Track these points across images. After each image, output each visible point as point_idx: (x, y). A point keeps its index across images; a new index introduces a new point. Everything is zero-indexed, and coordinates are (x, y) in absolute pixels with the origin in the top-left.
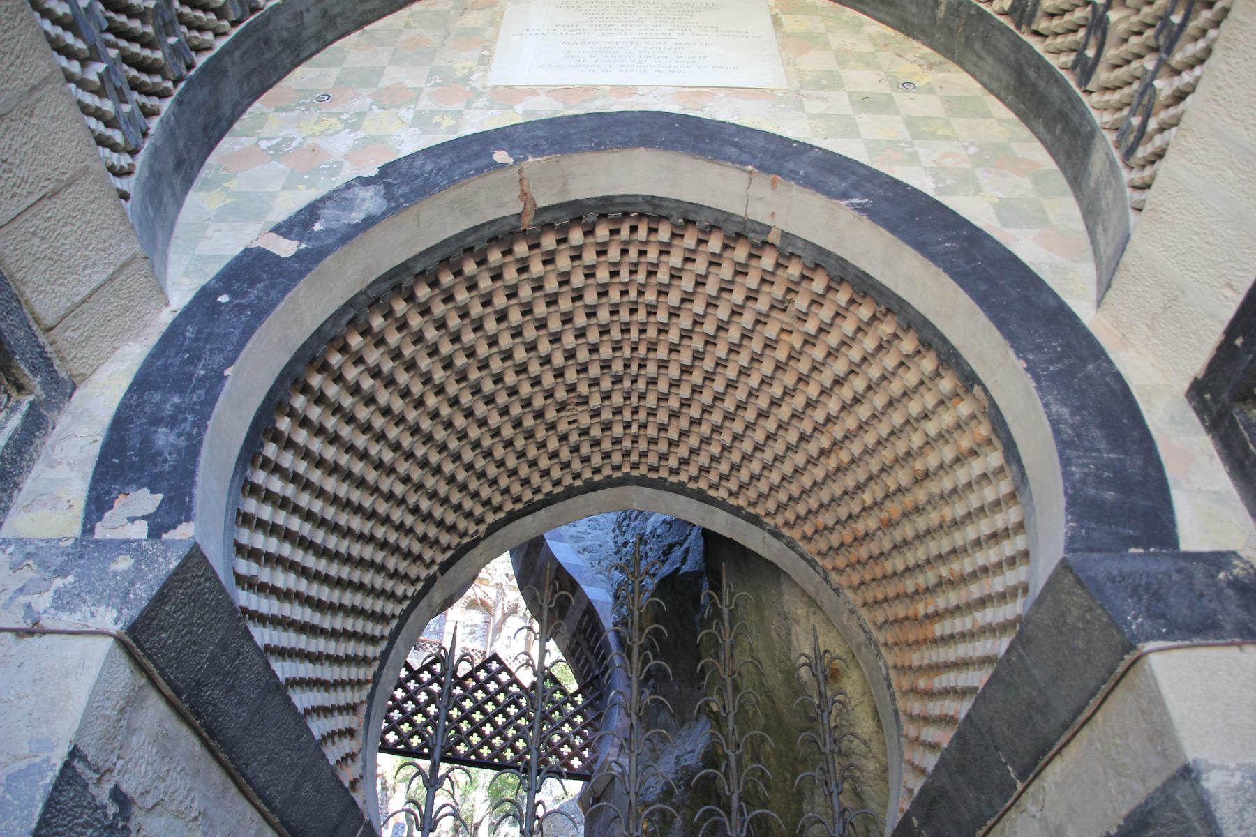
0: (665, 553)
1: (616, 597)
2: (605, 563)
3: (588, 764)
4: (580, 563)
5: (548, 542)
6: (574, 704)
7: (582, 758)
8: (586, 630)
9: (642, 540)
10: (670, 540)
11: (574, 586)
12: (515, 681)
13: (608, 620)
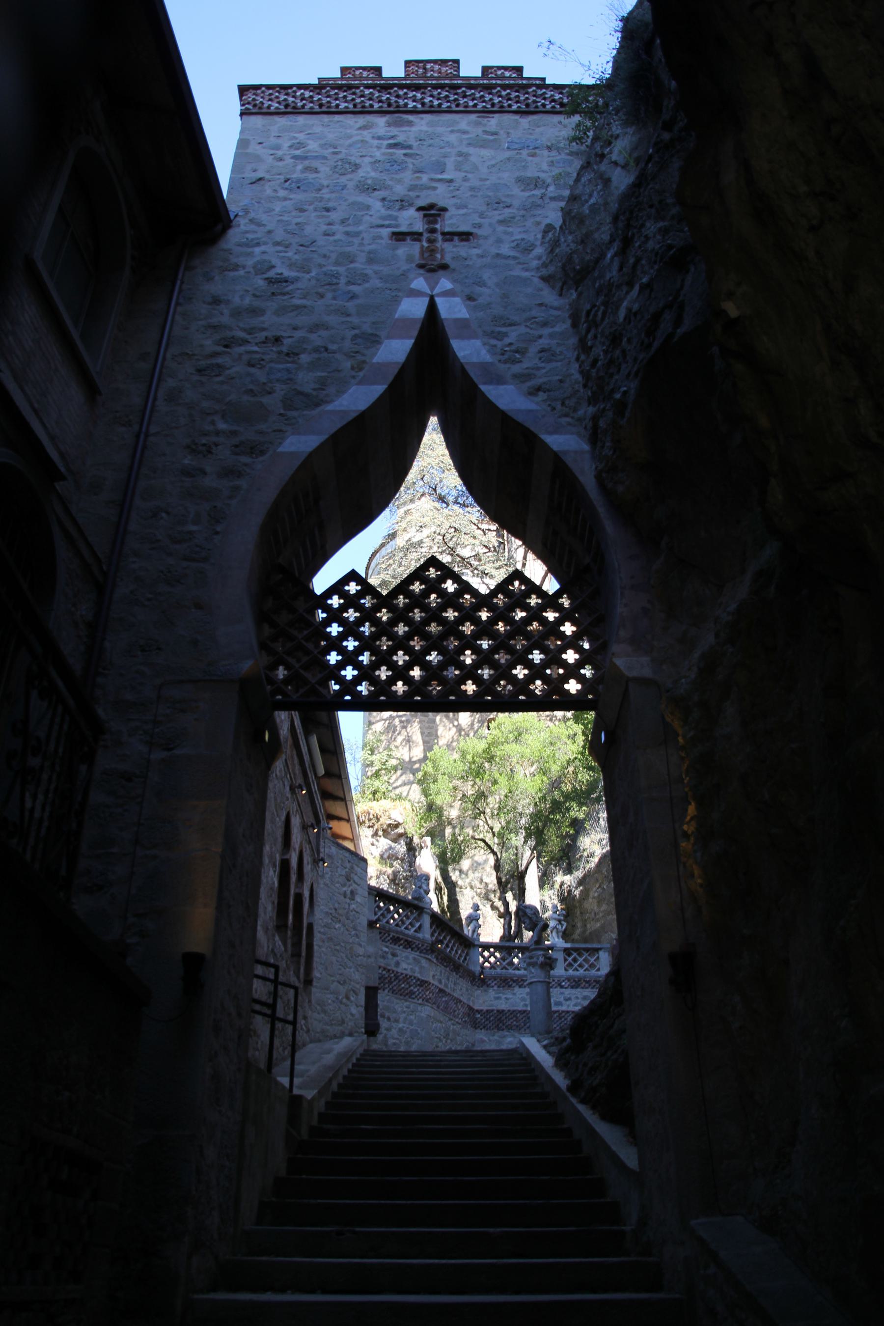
1: (594, 439)
2: (571, 403)
4: (533, 407)
5: (483, 388)
6: (558, 608)
7: (581, 679)
9: (615, 339)
12: (465, 587)
13: (586, 474)
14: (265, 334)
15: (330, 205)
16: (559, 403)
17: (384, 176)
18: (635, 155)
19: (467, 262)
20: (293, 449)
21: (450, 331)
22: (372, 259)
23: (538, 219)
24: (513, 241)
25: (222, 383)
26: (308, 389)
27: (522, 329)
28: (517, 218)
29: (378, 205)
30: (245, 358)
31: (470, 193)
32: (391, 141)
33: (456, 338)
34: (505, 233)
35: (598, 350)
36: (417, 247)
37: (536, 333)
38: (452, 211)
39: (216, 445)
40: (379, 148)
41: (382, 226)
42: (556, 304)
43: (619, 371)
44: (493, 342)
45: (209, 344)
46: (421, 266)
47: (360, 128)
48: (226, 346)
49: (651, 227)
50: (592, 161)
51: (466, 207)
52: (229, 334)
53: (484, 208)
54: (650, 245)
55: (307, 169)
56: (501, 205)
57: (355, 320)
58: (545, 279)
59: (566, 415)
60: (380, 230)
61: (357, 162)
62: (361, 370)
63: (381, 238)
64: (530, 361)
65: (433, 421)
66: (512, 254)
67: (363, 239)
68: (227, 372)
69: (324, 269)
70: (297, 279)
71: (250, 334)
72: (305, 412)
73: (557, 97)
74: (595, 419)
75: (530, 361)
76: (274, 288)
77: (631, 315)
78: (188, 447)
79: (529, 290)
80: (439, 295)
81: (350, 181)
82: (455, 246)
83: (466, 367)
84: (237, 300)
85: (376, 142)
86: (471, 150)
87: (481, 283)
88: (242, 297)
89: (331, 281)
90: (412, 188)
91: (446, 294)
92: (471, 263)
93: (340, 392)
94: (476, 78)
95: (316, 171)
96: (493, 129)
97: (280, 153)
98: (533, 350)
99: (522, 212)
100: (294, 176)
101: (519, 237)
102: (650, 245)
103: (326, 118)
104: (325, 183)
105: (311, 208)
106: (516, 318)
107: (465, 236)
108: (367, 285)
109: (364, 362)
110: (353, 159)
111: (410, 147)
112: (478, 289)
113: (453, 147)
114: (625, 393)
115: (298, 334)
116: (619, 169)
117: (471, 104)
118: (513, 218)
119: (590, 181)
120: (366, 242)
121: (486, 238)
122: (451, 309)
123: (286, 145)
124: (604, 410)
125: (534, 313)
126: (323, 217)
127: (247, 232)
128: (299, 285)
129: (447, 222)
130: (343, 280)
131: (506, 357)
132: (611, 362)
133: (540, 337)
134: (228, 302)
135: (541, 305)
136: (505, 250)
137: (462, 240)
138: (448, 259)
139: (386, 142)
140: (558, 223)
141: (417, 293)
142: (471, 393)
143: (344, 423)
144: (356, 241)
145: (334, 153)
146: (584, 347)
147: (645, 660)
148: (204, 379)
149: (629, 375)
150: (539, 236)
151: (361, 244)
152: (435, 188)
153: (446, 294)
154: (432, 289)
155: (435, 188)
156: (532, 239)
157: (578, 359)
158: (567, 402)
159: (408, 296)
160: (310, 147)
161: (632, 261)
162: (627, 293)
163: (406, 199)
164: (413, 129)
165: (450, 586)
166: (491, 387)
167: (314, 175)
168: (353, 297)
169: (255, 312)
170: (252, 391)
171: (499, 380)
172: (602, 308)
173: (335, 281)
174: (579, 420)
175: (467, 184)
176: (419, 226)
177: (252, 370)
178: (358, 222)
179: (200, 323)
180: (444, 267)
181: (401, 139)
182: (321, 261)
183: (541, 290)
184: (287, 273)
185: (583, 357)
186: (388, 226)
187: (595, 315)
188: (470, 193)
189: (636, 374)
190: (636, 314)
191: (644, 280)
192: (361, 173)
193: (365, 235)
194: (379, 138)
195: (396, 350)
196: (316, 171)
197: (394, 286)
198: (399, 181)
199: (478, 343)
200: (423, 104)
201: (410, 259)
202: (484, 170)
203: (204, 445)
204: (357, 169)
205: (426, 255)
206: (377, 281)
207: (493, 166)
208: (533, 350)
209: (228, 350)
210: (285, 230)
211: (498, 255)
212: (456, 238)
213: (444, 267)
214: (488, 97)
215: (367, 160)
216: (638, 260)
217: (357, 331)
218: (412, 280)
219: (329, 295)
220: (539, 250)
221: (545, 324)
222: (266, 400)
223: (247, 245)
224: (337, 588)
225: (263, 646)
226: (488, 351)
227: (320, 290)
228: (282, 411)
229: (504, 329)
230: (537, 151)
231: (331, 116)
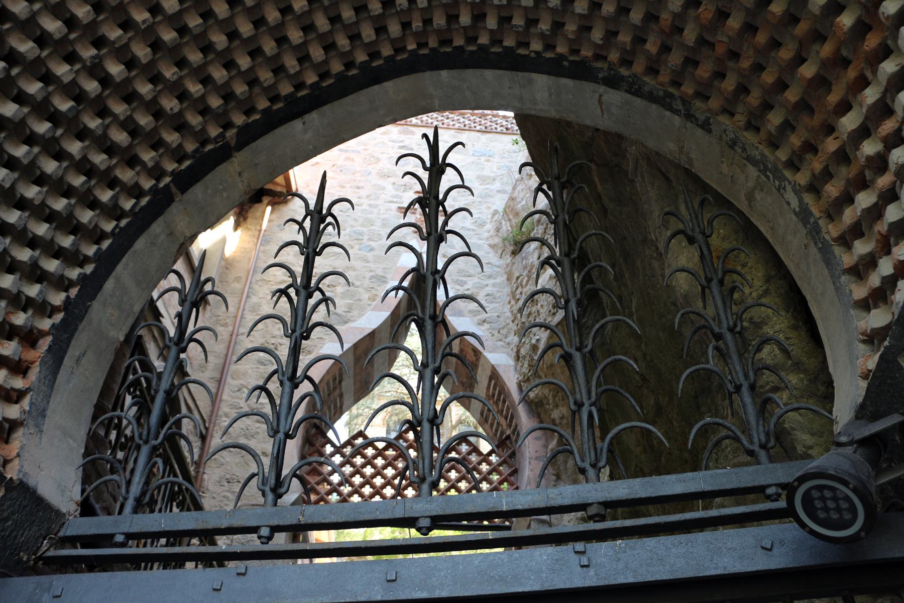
1: (518, 358)
2: (504, 332)
6: (489, 463)
8: (493, 395)
13: (511, 380)
15: (360, 185)
23: (489, 205)
27: (476, 280)
29: (391, 187)
32: (401, 144)
37: (485, 283)
41: (392, 202)
42: (498, 263)
55: (347, 159)
57: (372, 266)
58: (493, 246)
61: (379, 156)
62: (374, 300)
66: (472, 227)
73: (504, 123)
85: (391, 144)
93: (361, 315)
95: (353, 160)
99: (480, 199)
104: (358, 169)
105: (349, 185)
114: (538, 340)
117: (452, 123)
120: (381, 212)
130: (366, 237)
133: (487, 285)
139: (397, 145)
140: (501, 210)
143: (362, 336)
144: (375, 211)
145: (366, 149)
150: (490, 216)
151: (378, 214)
156: (484, 218)
157: (509, 303)
168: (372, 250)
173: (361, 237)
174: (508, 344)
178: (377, 198)
182: (353, 223)
183: (488, 253)
186: (396, 202)
187: (522, 281)
192: (381, 165)
194: (393, 141)
196: (353, 160)
214: (462, 120)
217: (372, 274)
219: (357, 247)
220: (488, 226)
227: (351, 243)
229: (464, 279)
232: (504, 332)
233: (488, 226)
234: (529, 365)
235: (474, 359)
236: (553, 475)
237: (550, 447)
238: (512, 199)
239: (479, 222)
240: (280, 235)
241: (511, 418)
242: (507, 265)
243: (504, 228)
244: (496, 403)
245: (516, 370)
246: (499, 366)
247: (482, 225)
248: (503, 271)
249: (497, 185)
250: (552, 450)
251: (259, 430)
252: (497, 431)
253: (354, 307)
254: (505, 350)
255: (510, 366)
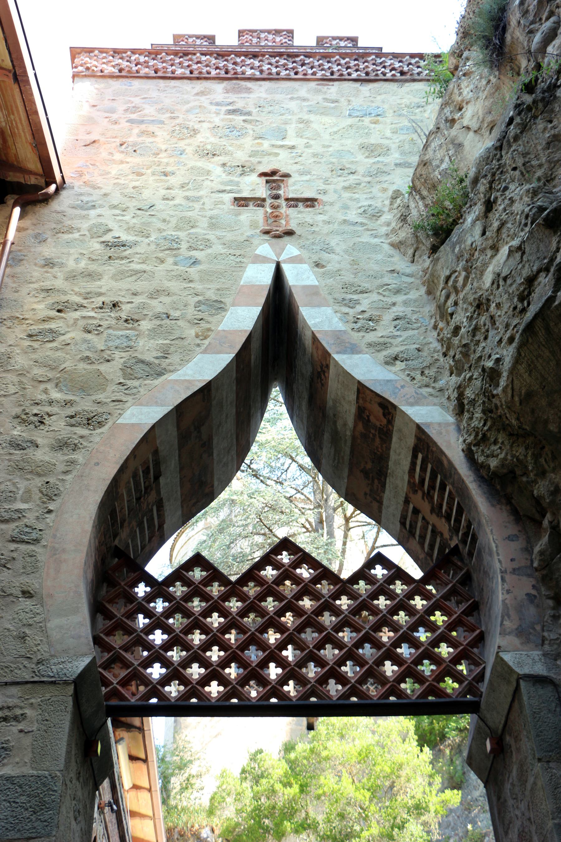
0: (522, 298)
1: (460, 408)
2: (431, 372)
3: (472, 686)
5: (336, 357)
7: (458, 677)
8: (422, 481)
9: (481, 305)
10: (526, 272)
11: (388, 409)
14: (101, 299)
15: (169, 169)
16: (419, 372)
17: (224, 142)
18: (489, 119)
19: (314, 228)
20: (134, 421)
21: (299, 298)
22: (213, 225)
23: (385, 186)
24: (360, 208)
25: (57, 349)
26: (148, 357)
28: (363, 185)
30: (81, 323)
31: (313, 160)
32: (230, 108)
33: (306, 306)
34: (351, 199)
35: (461, 317)
36: (261, 211)
37: (390, 300)
38: (295, 177)
39: (50, 416)
40: (218, 114)
41: (223, 191)
42: (408, 271)
43: (486, 338)
44: (346, 310)
45: (42, 308)
46: (267, 232)
47: (197, 94)
48: (59, 311)
49: (516, 190)
50: (442, 126)
51: (309, 173)
52: (64, 298)
53: (328, 174)
54: (518, 207)
55: (143, 133)
56: (346, 171)
57: (198, 286)
59: (427, 386)
60: (221, 195)
61: (196, 127)
62: (205, 338)
63: (223, 203)
64: (385, 329)
65: (276, 393)
66: (360, 220)
67: (203, 204)
68: (62, 338)
69: (164, 234)
70: (136, 243)
71: (86, 299)
72: (147, 382)
73: (397, 65)
74: (460, 389)
75: (385, 329)
76: (111, 252)
77: (499, 279)
78: (18, 417)
79: (379, 257)
80: (285, 261)
81: (189, 146)
82: (300, 212)
83: (318, 335)
84: (71, 264)
85: (214, 108)
86: (312, 117)
87: (329, 250)
88: (77, 260)
89: (172, 245)
90: (253, 154)
91: (293, 260)
92: (317, 229)
93: (184, 361)
94: (312, 48)
96: (334, 97)
97: (115, 116)
98: (388, 317)
99: (368, 179)
100: (131, 139)
101: (366, 203)
102: (518, 207)
103: (162, 83)
104: (163, 147)
105: (149, 171)
106: (366, 285)
107: (310, 202)
108: (209, 251)
109: (209, 330)
110: (191, 124)
111: (249, 114)
112: (325, 256)
113: (293, 114)
114: (498, 360)
115: (137, 300)
116: (471, 134)
117: (310, 71)
118: (359, 184)
119: (441, 146)
120: (207, 207)
121: (332, 204)
122: (297, 277)
123: (121, 108)
124: (471, 378)
125: (386, 280)
126: (162, 181)
127: (81, 194)
128: (138, 249)
129: (291, 188)
130: (184, 246)
131: (359, 325)
132: (476, 329)
133: (394, 304)
134: (62, 265)
135: (393, 271)
136: (353, 216)
137: (307, 206)
138: (293, 226)
139: (224, 109)
140: (405, 189)
141: (264, 260)
142: (322, 364)
143: (189, 393)
144: (197, 206)
145: (172, 118)
146: (444, 314)
147: (536, 654)
148: (36, 345)
149: (500, 341)
150: (387, 202)
151: (202, 209)
152: (277, 155)
153: (293, 260)
154: (278, 255)
155: (277, 155)
156: (379, 205)
157: (435, 327)
158: (426, 372)
159: (253, 263)
160: (146, 111)
161: (496, 224)
162: (492, 257)
163: (247, 164)
164: (251, 96)
165: (305, 572)
166: (344, 356)
167: (151, 140)
168: (196, 262)
169: (90, 276)
170: (88, 358)
171: (353, 349)
172: (464, 274)
173: (176, 246)
174: (441, 390)
175: (310, 151)
176: (262, 191)
177: (89, 336)
178: (199, 187)
179: (32, 286)
180: (290, 233)
181: (240, 105)
183: (392, 256)
184: (125, 237)
185: (441, 325)
186: (230, 192)
187: (456, 281)
188: (313, 160)
189: (511, 340)
190: (505, 279)
191: (516, 243)
192: (200, 138)
193: (206, 200)
194: (217, 104)
195: (243, 318)
197: (238, 252)
198: (240, 147)
199: (329, 311)
200: (261, 72)
201: (253, 225)
202: (327, 137)
203: (36, 415)
204: (195, 134)
205: (270, 221)
206: (220, 247)
207: (336, 133)
208: (388, 317)
209: (62, 315)
210: (122, 194)
211: (345, 221)
212: (300, 204)
213: (290, 233)
214: (327, 66)
215: (205, 125)
216: (503, 224)
217: (200, 298)
218: (257, 247)
219: (170, 260)
220: (387, 217)
221: (398, 291)
222: (104, 368)
223: (82, 208)
224: (179, 575)
225: (97, 640)
226: (341, 319)
227: (161, 255)
228: (122, 381)
229: (355, 297)
230: (379, 118)
231: (168, 81)
232: (431, 372)
233: (387, 217)
234: (484, 412)
235: (385, 421)
236: (548, 597)
237: (537, 549)
238: (424, 164)
239: (370, 211)
240: (39, 249)
241: (458, 512)
242: (425, 271)
243: (414, 213)
244: (428, 496)
245: (459, 430)
246: (429, 425)
247: (376, 215)
248: (418, 282)
249: (395, 156)
250: (541, 553)
251: (15, 555)
252: (432, 546)
253: (172, 349)
254: (436, 400)
255: (448, 424)
